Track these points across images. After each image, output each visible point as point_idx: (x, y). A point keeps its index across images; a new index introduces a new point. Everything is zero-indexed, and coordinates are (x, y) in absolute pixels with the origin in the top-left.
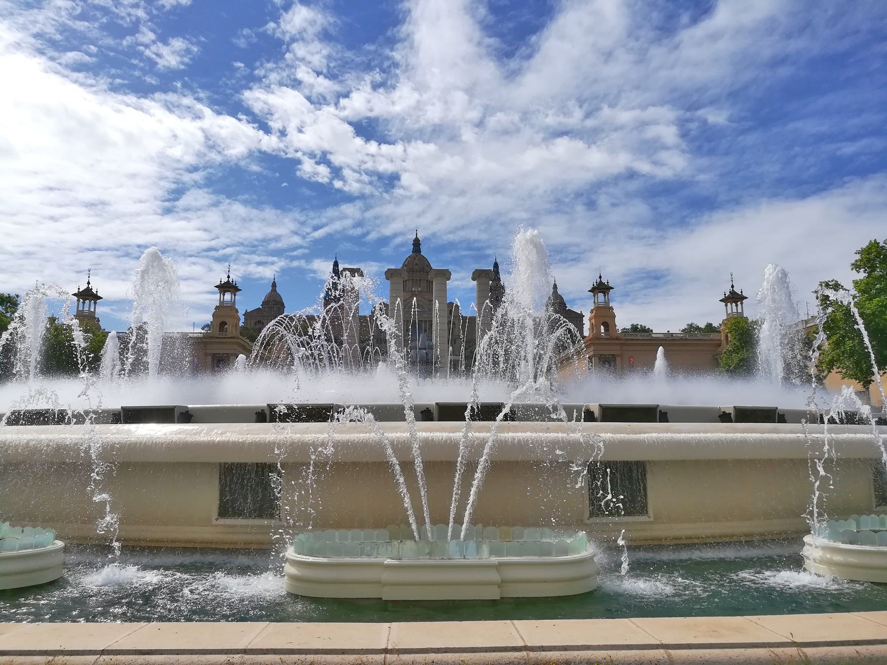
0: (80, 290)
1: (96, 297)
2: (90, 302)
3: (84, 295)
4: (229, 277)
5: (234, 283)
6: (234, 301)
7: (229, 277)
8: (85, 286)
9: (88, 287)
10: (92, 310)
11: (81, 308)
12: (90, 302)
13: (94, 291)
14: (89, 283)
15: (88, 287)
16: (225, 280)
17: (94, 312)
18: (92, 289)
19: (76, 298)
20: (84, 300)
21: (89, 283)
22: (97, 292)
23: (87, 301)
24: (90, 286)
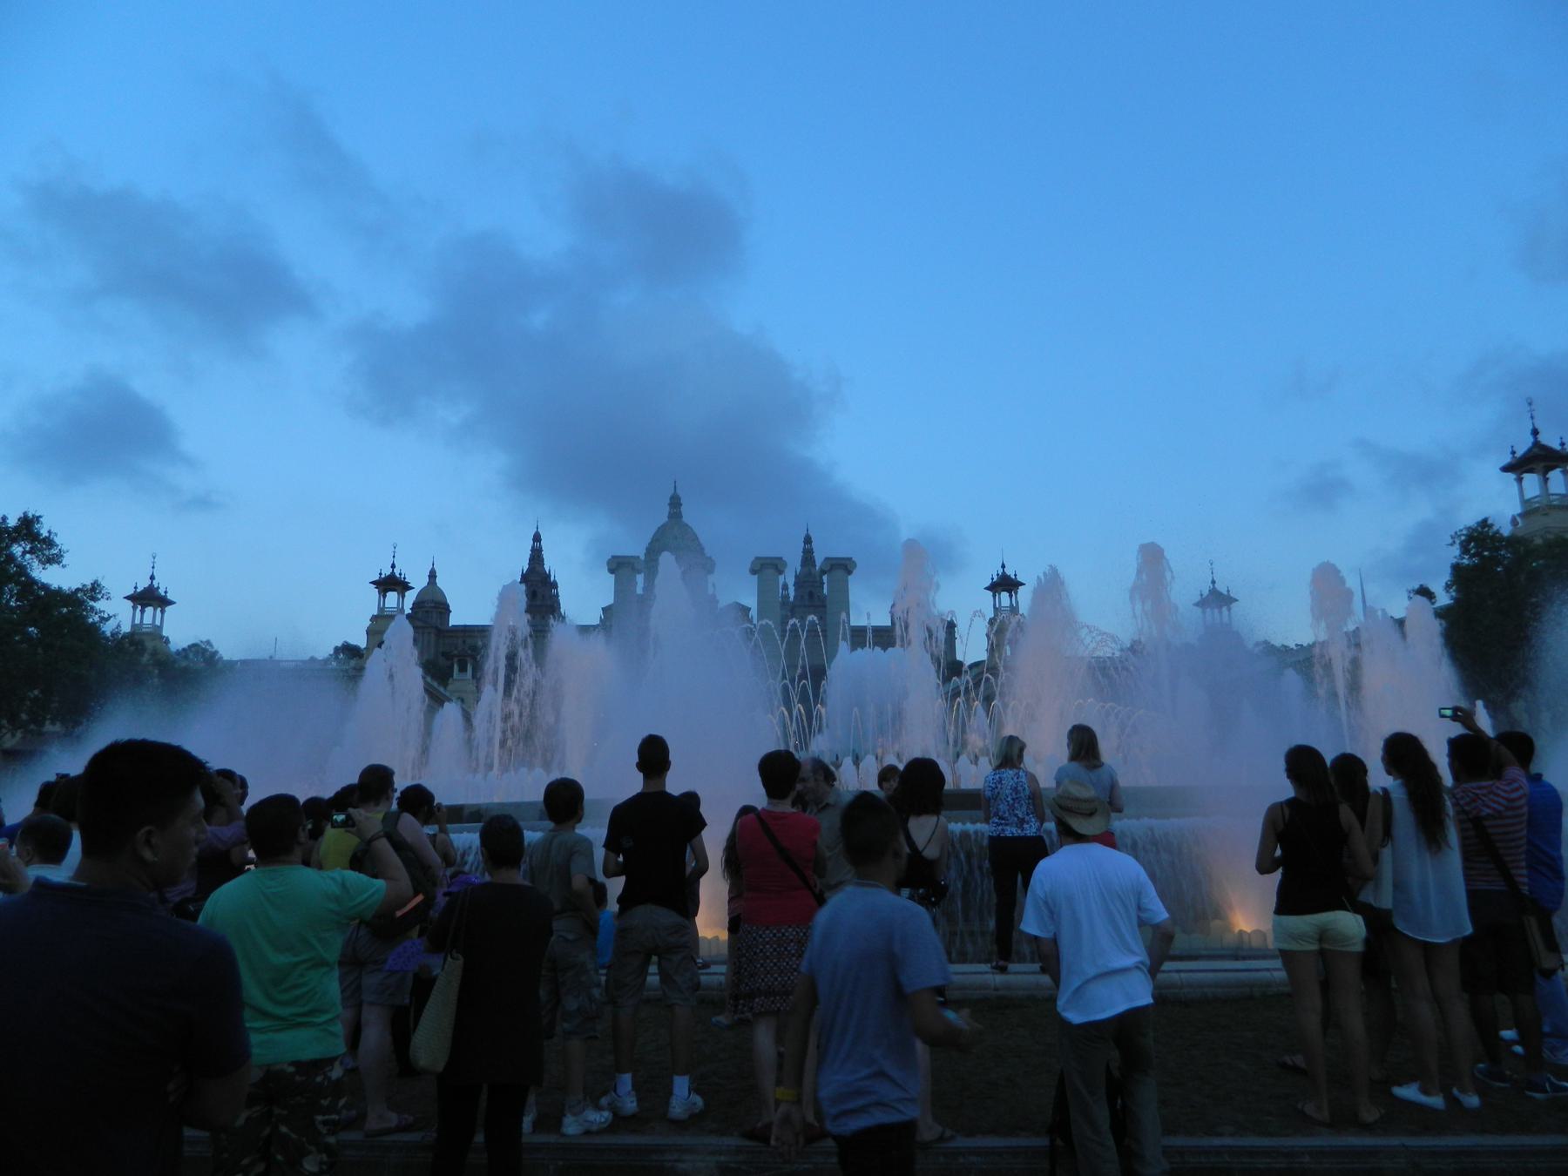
0: (138, 590)
1: (162, 602)
2: (155, 610)
4: (393, 566)
5: (403, 576)
6: (403, 607)
7: (393, 566)
8: (146, 583)
9: (151, 585)
10: (158, 623)
11: (137, 621)
12: (155, 610)
13: (162, 592)
14: (152, 578)
15: (151, 585)
16: (387, 571)
17: (160, 627)
18: (158, 588)
19: (130, 604)
21: (152, 578)
22: (166, 592)
23: (149, 610)
24: (155, 584)
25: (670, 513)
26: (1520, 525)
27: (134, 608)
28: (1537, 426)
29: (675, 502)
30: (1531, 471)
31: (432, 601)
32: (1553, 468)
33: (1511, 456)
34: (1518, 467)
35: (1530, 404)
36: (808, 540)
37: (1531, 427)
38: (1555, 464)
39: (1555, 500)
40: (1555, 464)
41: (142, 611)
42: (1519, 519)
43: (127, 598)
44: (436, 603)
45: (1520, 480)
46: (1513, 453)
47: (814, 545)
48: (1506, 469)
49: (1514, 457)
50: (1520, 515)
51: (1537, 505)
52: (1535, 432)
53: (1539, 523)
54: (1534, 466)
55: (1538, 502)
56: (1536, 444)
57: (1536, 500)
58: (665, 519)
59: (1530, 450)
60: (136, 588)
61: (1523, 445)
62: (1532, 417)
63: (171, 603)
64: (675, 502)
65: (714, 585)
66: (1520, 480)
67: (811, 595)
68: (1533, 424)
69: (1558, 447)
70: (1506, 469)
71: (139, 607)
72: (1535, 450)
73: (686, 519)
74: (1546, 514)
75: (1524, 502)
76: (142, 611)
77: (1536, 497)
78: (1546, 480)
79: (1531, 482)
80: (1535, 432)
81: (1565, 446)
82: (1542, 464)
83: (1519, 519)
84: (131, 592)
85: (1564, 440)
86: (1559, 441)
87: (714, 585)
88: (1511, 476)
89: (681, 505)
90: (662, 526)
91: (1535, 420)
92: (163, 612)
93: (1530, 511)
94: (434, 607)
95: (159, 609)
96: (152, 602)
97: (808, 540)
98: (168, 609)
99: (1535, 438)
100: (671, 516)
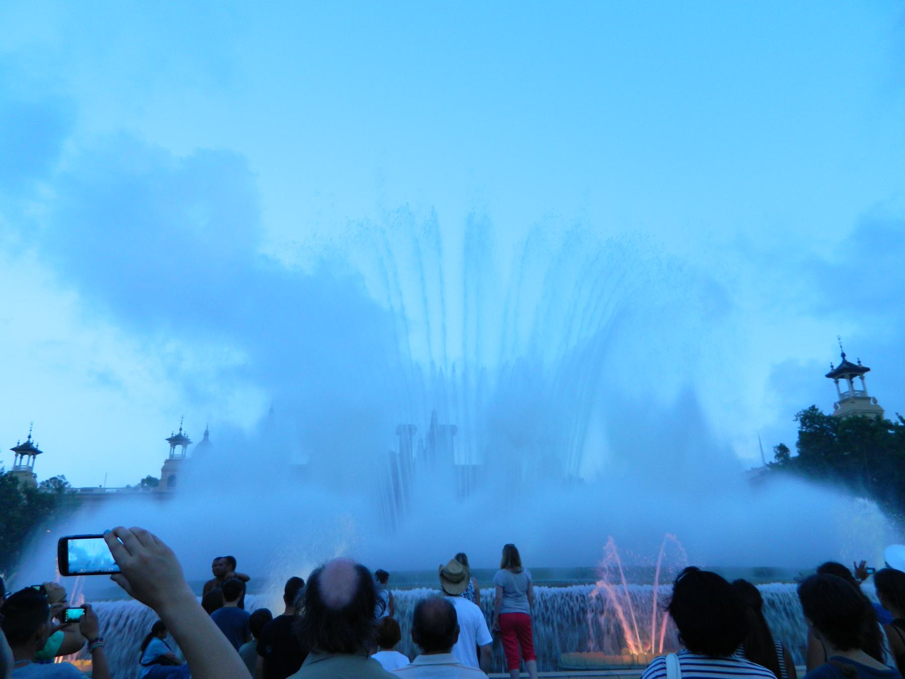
0: (20, 445)
3: (25, 450)
4: (181, 429)
5: (186, 435)
7: (181, 429)
9: (28, 442)
11: (17, 464)
12: (30, 456)
13: (35, 445)
16: (177, 433)
17: (31, 468)
18: (32, 443)
19: (14, 453)
20: (22, 454)
21: (29, 437)
22: (37, 446)
23: (26, 457)
24: (31, 441)
26: (839, 408)
27: (16, 456)
28: (844, 352)
30: (843, 377)
32: (855, 376)
33: (831, 368)
34: (836, 374)
35: (839, 339)
37: (841, 352)
38: (855, 373)
39: (858, 394)
40: (855, 373)
41: (21, 458)
42: (838, 405)
43: (13, 449)
45: (837, 382)
46: (832, 367)
48: (829, 376)
49: (833, 369)
50: (840, 403)
51: (847, 397)
52: (843, 355)
53: (849, 408)
54: (843, 374)
55: (848, 395)
56: (844, 362)
57: (848, 393)
59: (841, 365)
60: (18, 443)
61: (837, 362)
62: (841, 347)
63: (39, 452)
66: (837, 382)
68: (842, 352)
69: (857, 364)
70: (829, 376)
71: (20, 455)
72: (844, 365)
74: (854, 402)
75: (841, 395)
76: (21, 458)
77: (848, 392)
78: (852, 382)
79: (843, 383)
80: (843, 355)
81: (861, 363)
82: (849, 373)
83: (838, 405)
84: (15, 446)
85: (860, 360)
86: (857, 360)
88: (832, 380)
91: (843, 348)
92: (34, 458)
93: (844, 400)
95: (32, 456)
96: (29, 452)
98: (38, 456)
99: (844, 358)
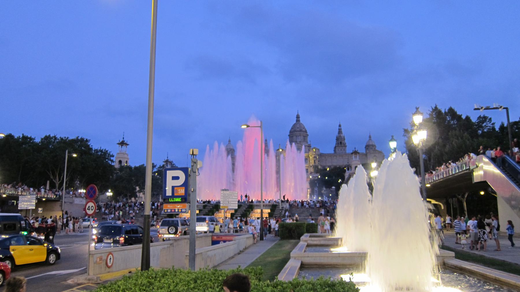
25: (297, 120)
29: (298, 117)
31: (230, 149)
36: (340, 126)
44: (231, 149)
47: (342, 127)
58: (295, 122)
64: (298, 117)
65: (310, 141)
67: (341, 143)
73: (301, 122)
87: (310, 141)
89: (299, 117)
90: (294, 124)
94: (230, 150)
97: (340, 126)
100: (296, 121)
